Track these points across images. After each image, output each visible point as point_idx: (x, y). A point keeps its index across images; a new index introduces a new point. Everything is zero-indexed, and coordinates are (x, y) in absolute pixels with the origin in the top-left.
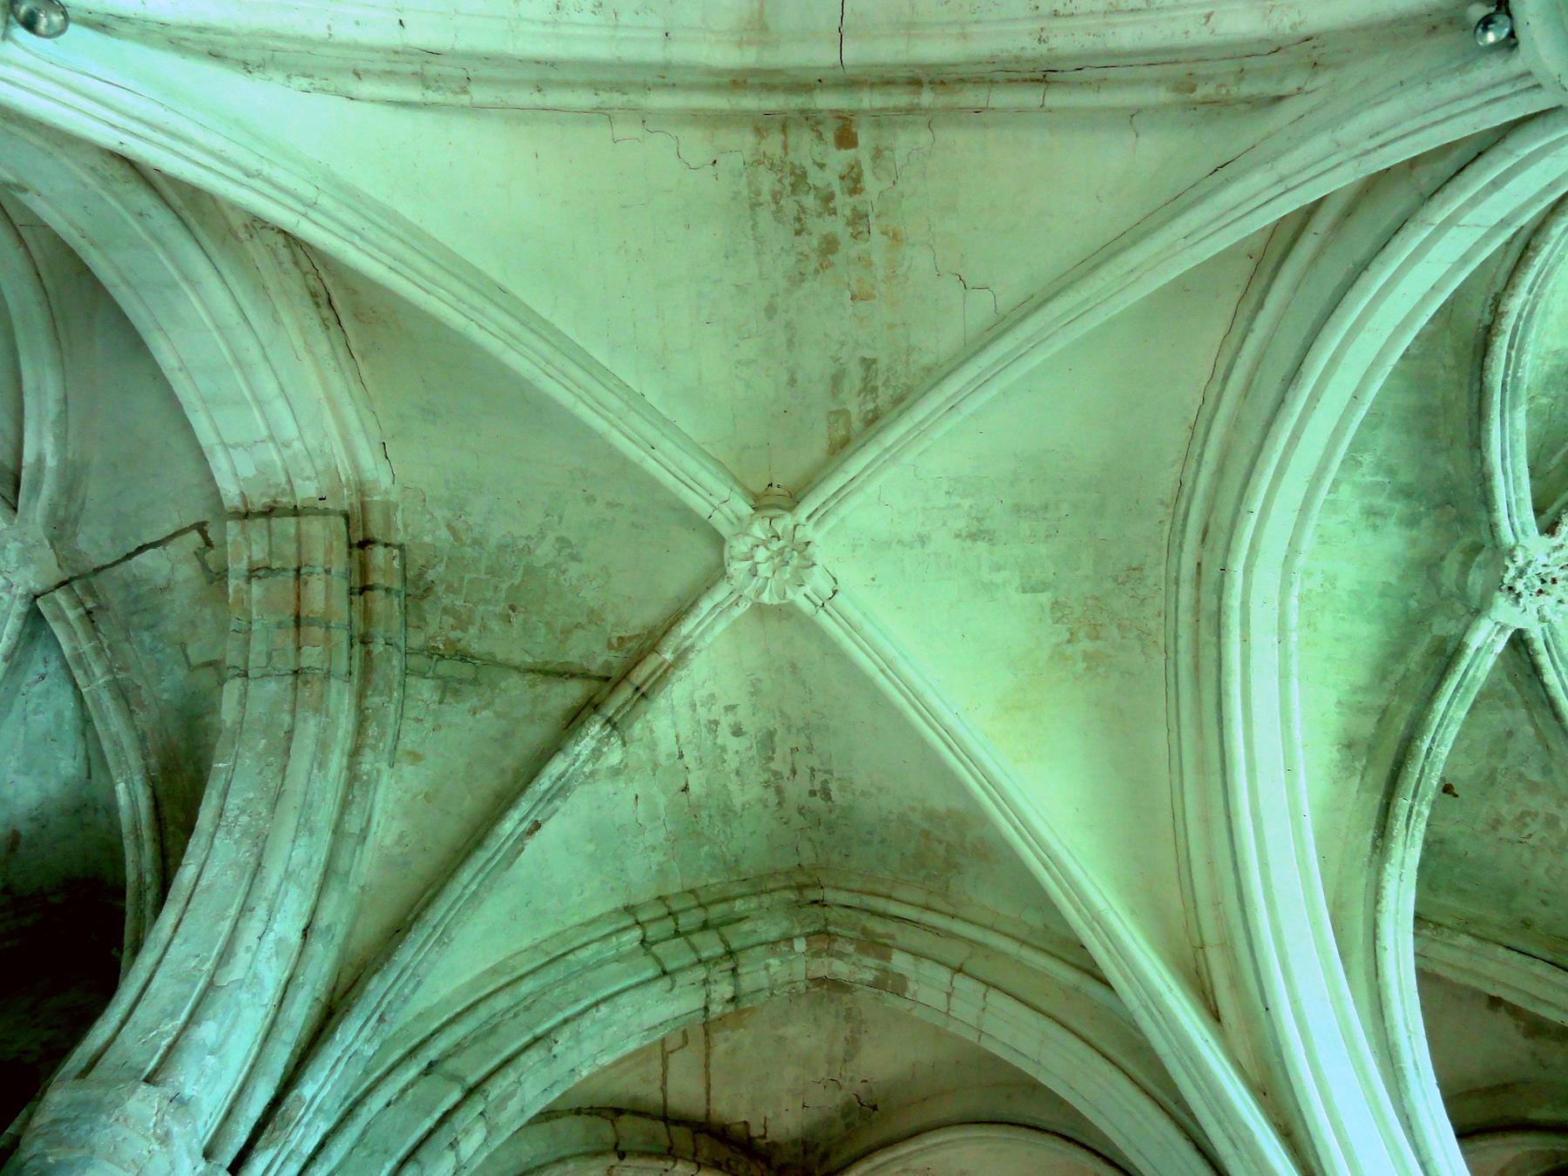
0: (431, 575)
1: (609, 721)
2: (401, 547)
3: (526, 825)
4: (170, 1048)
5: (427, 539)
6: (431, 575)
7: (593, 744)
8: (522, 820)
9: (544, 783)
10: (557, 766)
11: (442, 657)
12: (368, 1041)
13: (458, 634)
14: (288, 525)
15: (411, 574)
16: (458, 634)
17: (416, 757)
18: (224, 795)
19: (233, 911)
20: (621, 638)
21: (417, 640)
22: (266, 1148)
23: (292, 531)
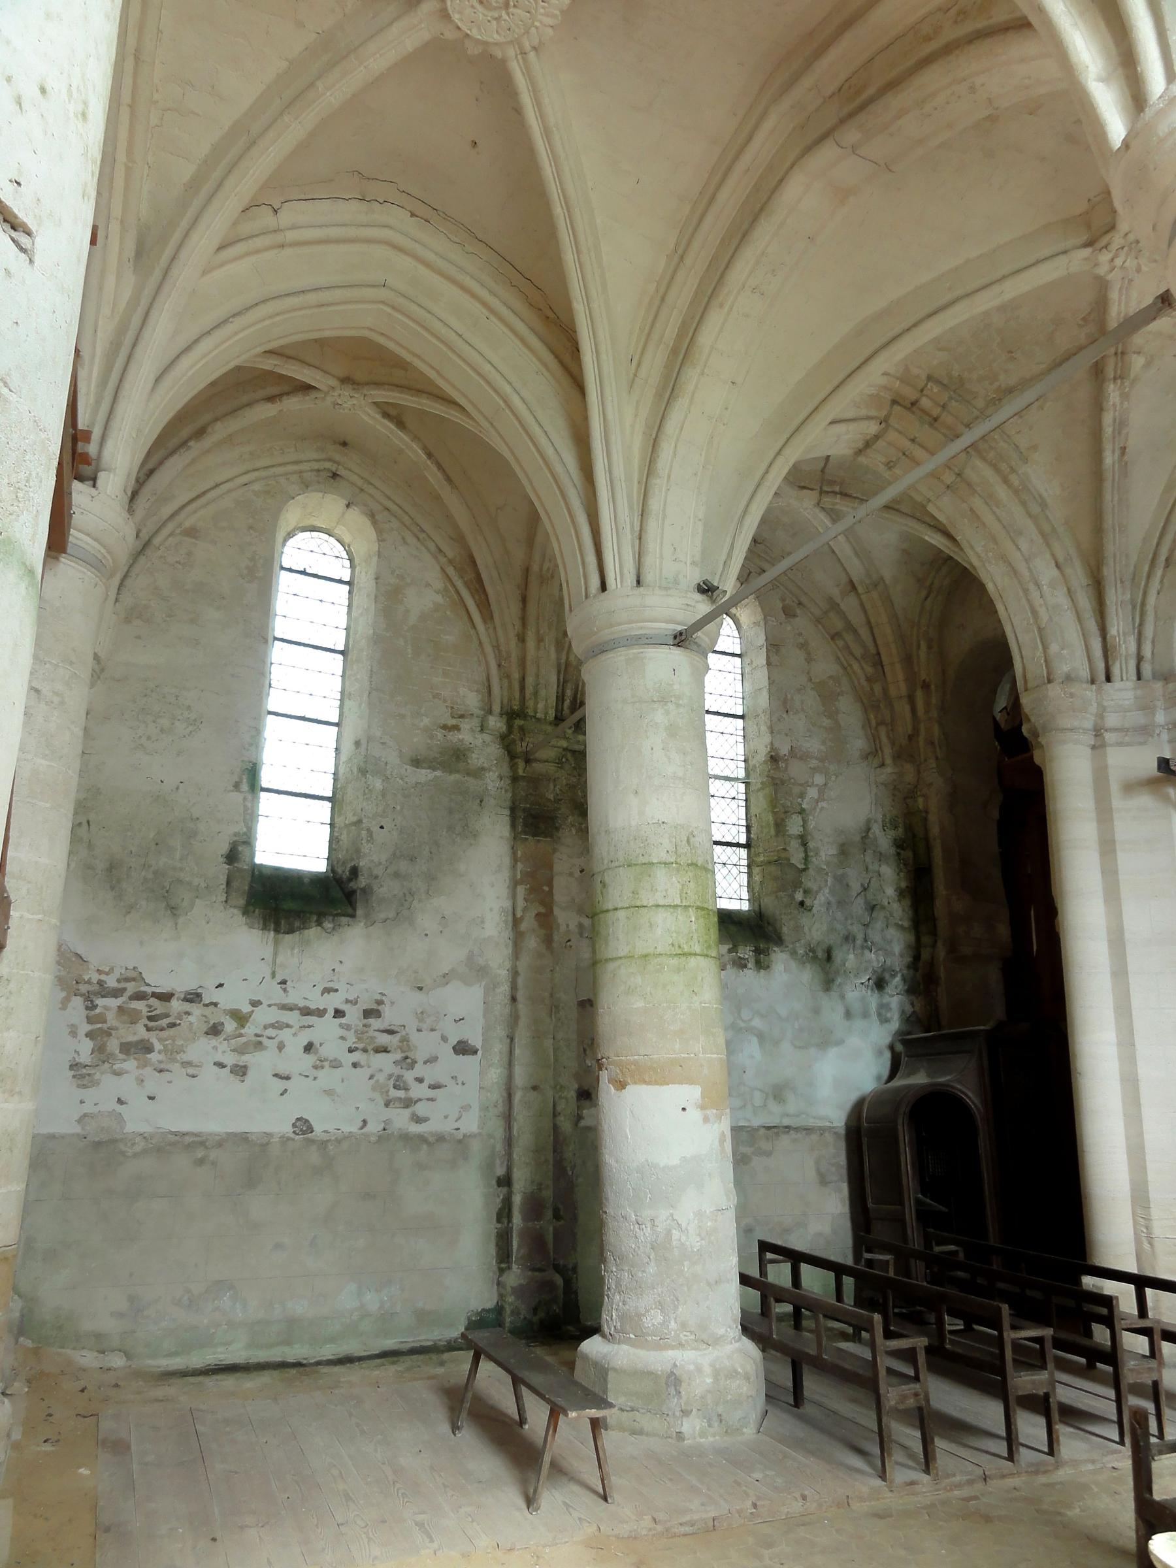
0: (955, 374)
1: (1115, 379)
2: (929, 378)
3: (1117, 453)
4: (1046, 661)
5: (935, 362)
6: (955, 374)
7: (1118, 393)
8: (1113, 452)
9: (1108, 431)
10: (1108, 419)
11: (1000, 400)
12: (1123, 593)
13: (996, 384)
14: (881, 444)
15: (945, 382)
16: (996, 384)
17: (1035, 448)
18: (972, 547)
19: (1021, 593)
20: (1084, 319)
21: (980, 403)
22: (1114, 663)
23: (884, 444)
